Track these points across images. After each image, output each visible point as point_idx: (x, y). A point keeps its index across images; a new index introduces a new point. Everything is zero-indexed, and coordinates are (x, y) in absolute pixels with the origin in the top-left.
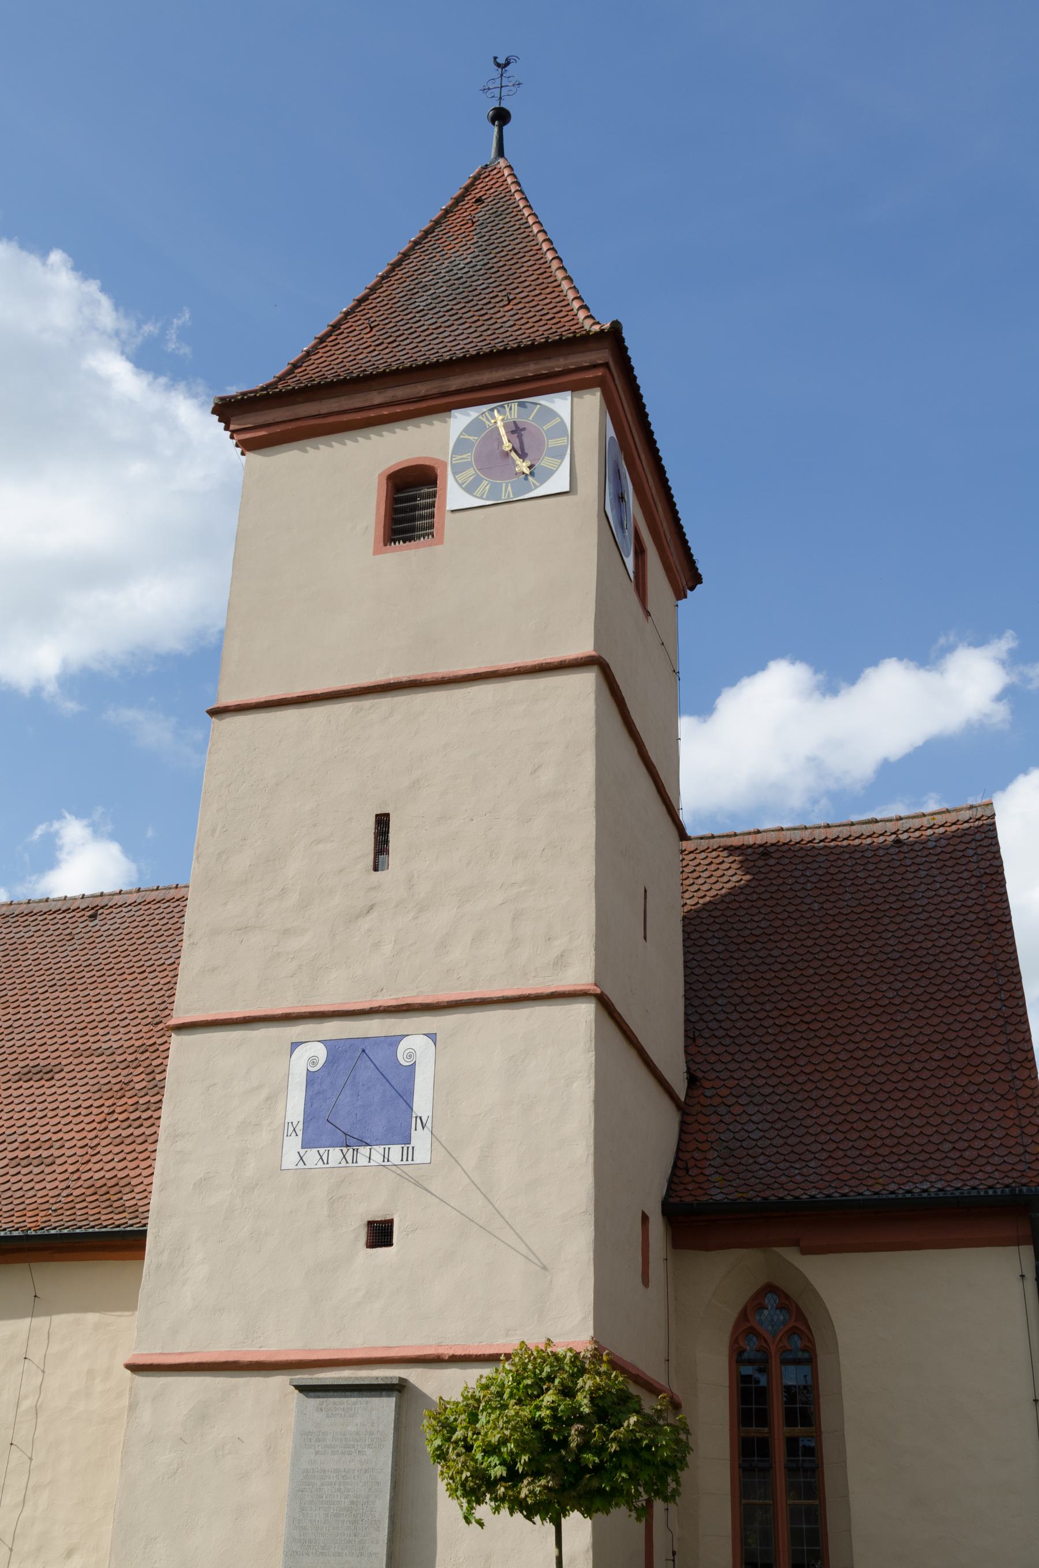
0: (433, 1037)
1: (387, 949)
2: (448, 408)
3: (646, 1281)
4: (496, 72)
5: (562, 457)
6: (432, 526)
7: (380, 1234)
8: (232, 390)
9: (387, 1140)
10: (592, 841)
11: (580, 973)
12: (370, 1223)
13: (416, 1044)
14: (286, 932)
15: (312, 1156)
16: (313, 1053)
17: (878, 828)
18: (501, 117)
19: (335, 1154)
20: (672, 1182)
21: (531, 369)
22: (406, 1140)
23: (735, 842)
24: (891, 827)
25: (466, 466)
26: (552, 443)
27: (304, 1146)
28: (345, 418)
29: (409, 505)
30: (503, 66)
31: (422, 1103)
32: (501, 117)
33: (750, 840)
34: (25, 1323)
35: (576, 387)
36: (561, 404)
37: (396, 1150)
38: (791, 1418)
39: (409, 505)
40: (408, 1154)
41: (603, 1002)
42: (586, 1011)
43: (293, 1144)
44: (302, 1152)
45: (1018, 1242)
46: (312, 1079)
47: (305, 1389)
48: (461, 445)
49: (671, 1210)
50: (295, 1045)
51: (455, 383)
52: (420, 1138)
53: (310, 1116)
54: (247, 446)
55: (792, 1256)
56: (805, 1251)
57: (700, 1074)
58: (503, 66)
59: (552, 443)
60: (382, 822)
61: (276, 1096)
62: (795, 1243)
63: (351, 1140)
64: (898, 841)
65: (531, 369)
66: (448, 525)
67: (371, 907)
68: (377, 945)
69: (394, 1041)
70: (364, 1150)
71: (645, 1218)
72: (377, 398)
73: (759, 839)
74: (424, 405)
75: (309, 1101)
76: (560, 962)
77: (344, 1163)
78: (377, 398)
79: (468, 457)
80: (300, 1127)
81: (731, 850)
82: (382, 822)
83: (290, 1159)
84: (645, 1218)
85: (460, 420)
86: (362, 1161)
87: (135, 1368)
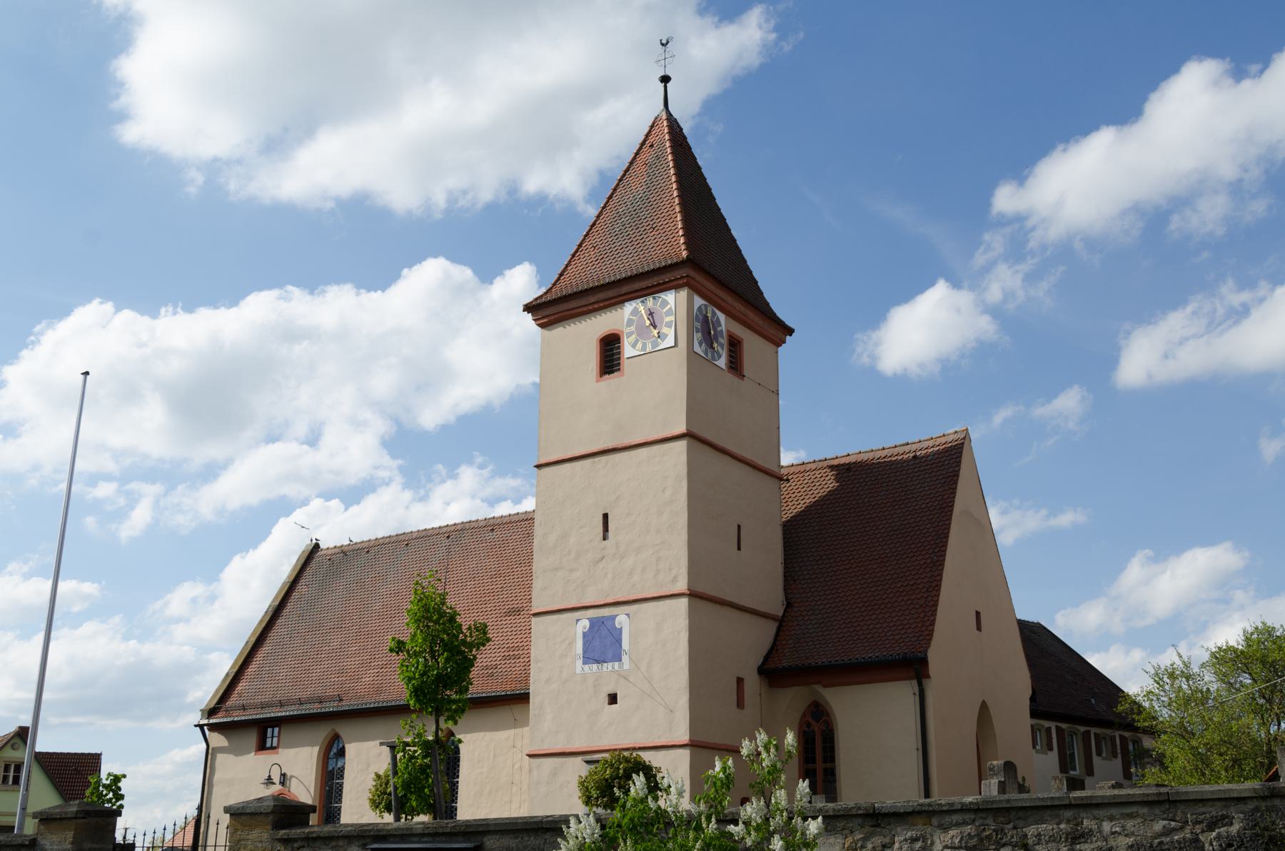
1: (610, 576)
2: (623, 302)
3: (740, 704)
7: (613, 699)
10: (686, 523)
11: (682, 586)
13: (622, 618)
14: (572, 570)
16: (584, 624)
17: (907, 448)
18: (665, 79)
19: (595, 666)
20: (766, 658)
23: (836, 462)
24: (914, 447)
25: (632, 333)
26: (668, 319)
29: (609, 354)
31: (625, 644)
32: (665, 79)
33: (843, 461)
34: (511, 732)
35: (677, 287)
36: (670, 297)
38: (825, 761)
39: (609, 354)
41: (693, 595)
42: (684, 602)
43: (579, 662)
45: (910, 679)
46: (585, 635)
47: (588, 762)
48: (630, 322)
49: (762, 671)
51: (625, 289)
52: (625, 658)
53: (585, 651)
54: (542, 326)
55: (819, 688)
56: (825, 686)
60: (606, 516)
61: (572, 644)
62: (819, 683)
63: (597, 662)
64: (915, 457)
66: (626, 364)
69: (613, 618)
71: (740, 681)
72: (592, 299)
73: (847, 460)
75: (584, 644)
76: (675, 580)
79: (633, 328)
81: (832, 467)
82: (606, 516)
83: (578, 670)
84: (740, 681)
85: (629, 307)
87: (530, 756)
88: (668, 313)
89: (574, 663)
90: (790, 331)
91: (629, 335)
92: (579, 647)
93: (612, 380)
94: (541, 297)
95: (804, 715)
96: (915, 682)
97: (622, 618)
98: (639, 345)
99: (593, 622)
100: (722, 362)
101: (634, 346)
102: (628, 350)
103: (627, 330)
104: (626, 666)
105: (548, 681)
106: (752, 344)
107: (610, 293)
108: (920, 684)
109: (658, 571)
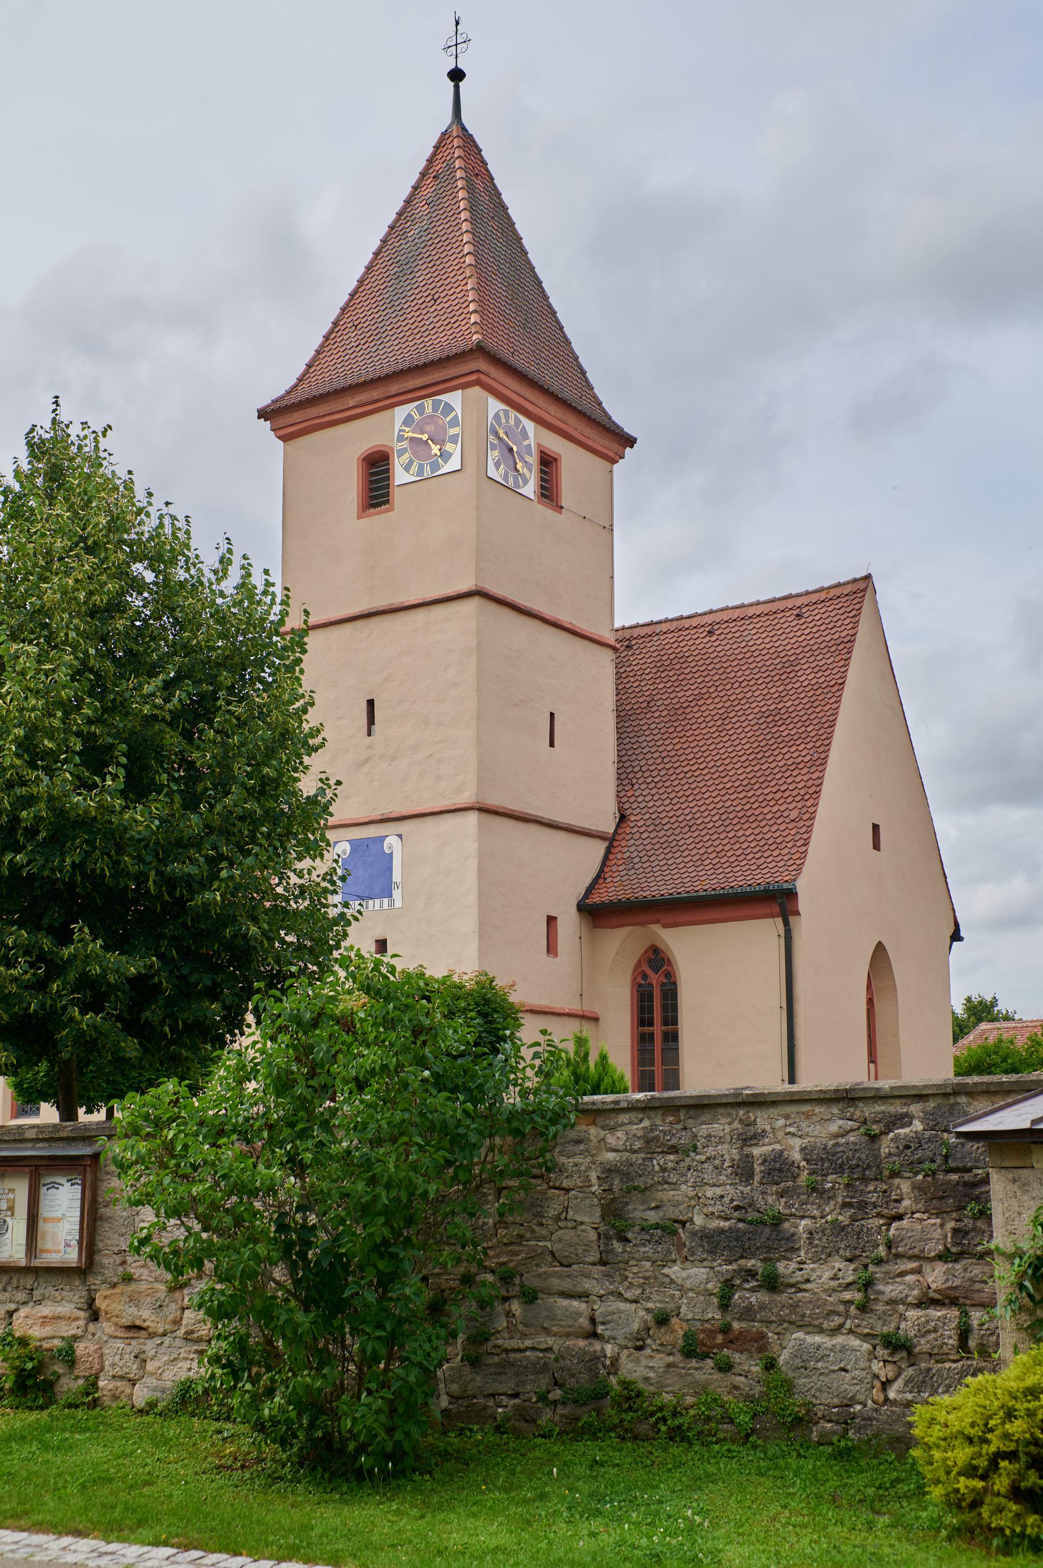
0: (400, 836)
2: (393, 406)
5: (456, 443)
6: (387, 494)
8: (265, 401)
9: (380, 896)
12: (376, 941)
18: (457, 75)
22: (390, 895)
25: (404, 451)
26: (453, 431)
31: (397, 876)
32: (457, 75)
35: (464, 386)
37: (386, 900)
38: (665, 1023)
40: (391, 904)
49: (583, 908)
51: (394, 388)
52: (397, 894)
54: (284, 438)
55: (657, 928)
56: (666, 926)
57: (629, 812)
59: (453, 431)
60: (371, 703)
62: (658, 922)
66: (397, 496)
67: (368, 759)
70: (371, 902)
71: (551, 920)
82: (371, 703)
84: (551, 920)
85: (401, 412)
88: (454, 423)
90: (631, 441)
94: (282, 397)
95: (639, 964)
96: (779, 921)
98: (415, 468)
99: (355, 844)
100: (530, 489)
101: (407, 468)
102: (400, 476)
103: (398, 446)
104: (398, 904)
106: (574, 462)
107: (375, 394)
108: (786, 923)
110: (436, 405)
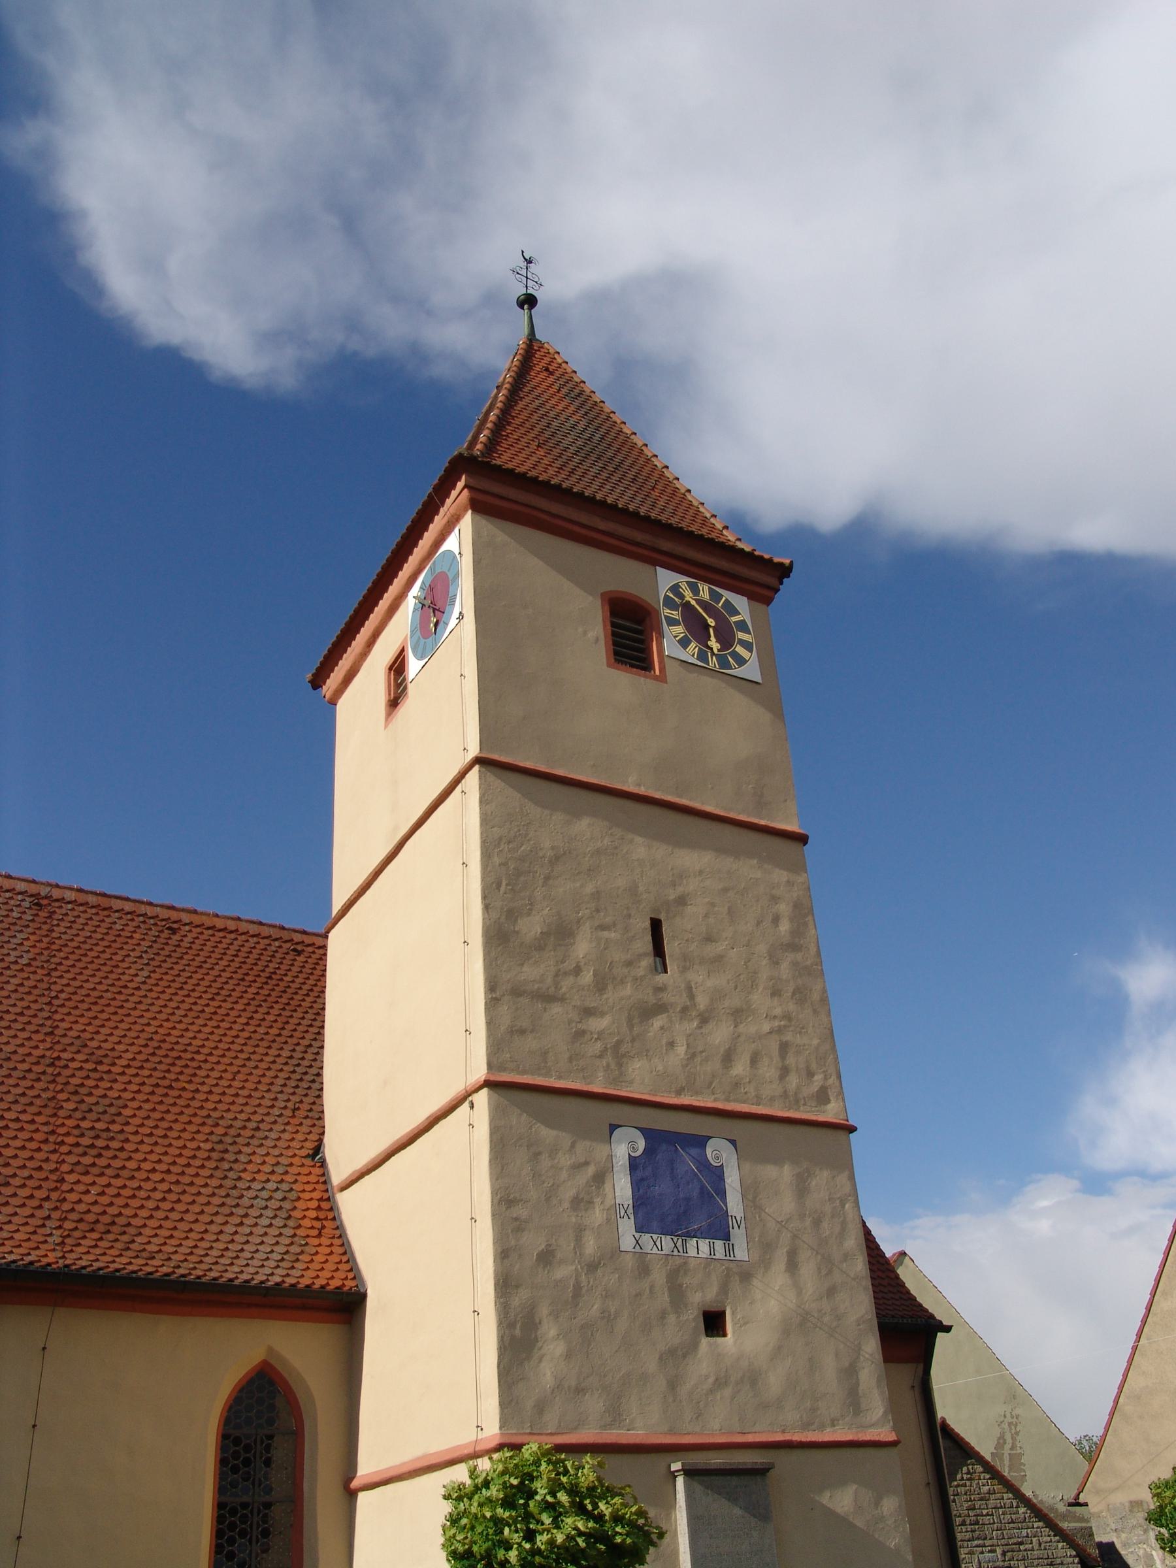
0: (733, 1142)
2: (655, 563)
4: (524, 264)
14: (588, 1012)
15: (646, 1238)
19: (667, 1242)
21: (724, 564)
22: (727, 1237)
27: (640, 1229)
28: (577, 529)
30: (529, 261)
31: (734, 1204)
37: (719, 1244)
40: (730, 1249)
43: (627, 1227)
44: (637, 1235)
50: (613, 1128)
51: (666, 545)
52: (738, 1236)
53: (641, 1202)
58: (529, 261)
60: (656, 926)
65: (724, 564)
66: (672, 669)
68: (671, 1044)
69: (701, 1142)
74: (640, 551)
75: (636, 1184)
77: (676, 1253)
78: (602, 525)
80: (630, 1210)
82: (656, 926)
85: (666, 579)
86: (692, 1252)
89: (611, 1223)
91: (672, 622)
92: (622, 1188)
93: (625, 681)
97: (718, 1151)
101: (684, 643)
104: (741, 1253)
105: (546, 1257)
109: (784, 1072)
110: (716, 597)
